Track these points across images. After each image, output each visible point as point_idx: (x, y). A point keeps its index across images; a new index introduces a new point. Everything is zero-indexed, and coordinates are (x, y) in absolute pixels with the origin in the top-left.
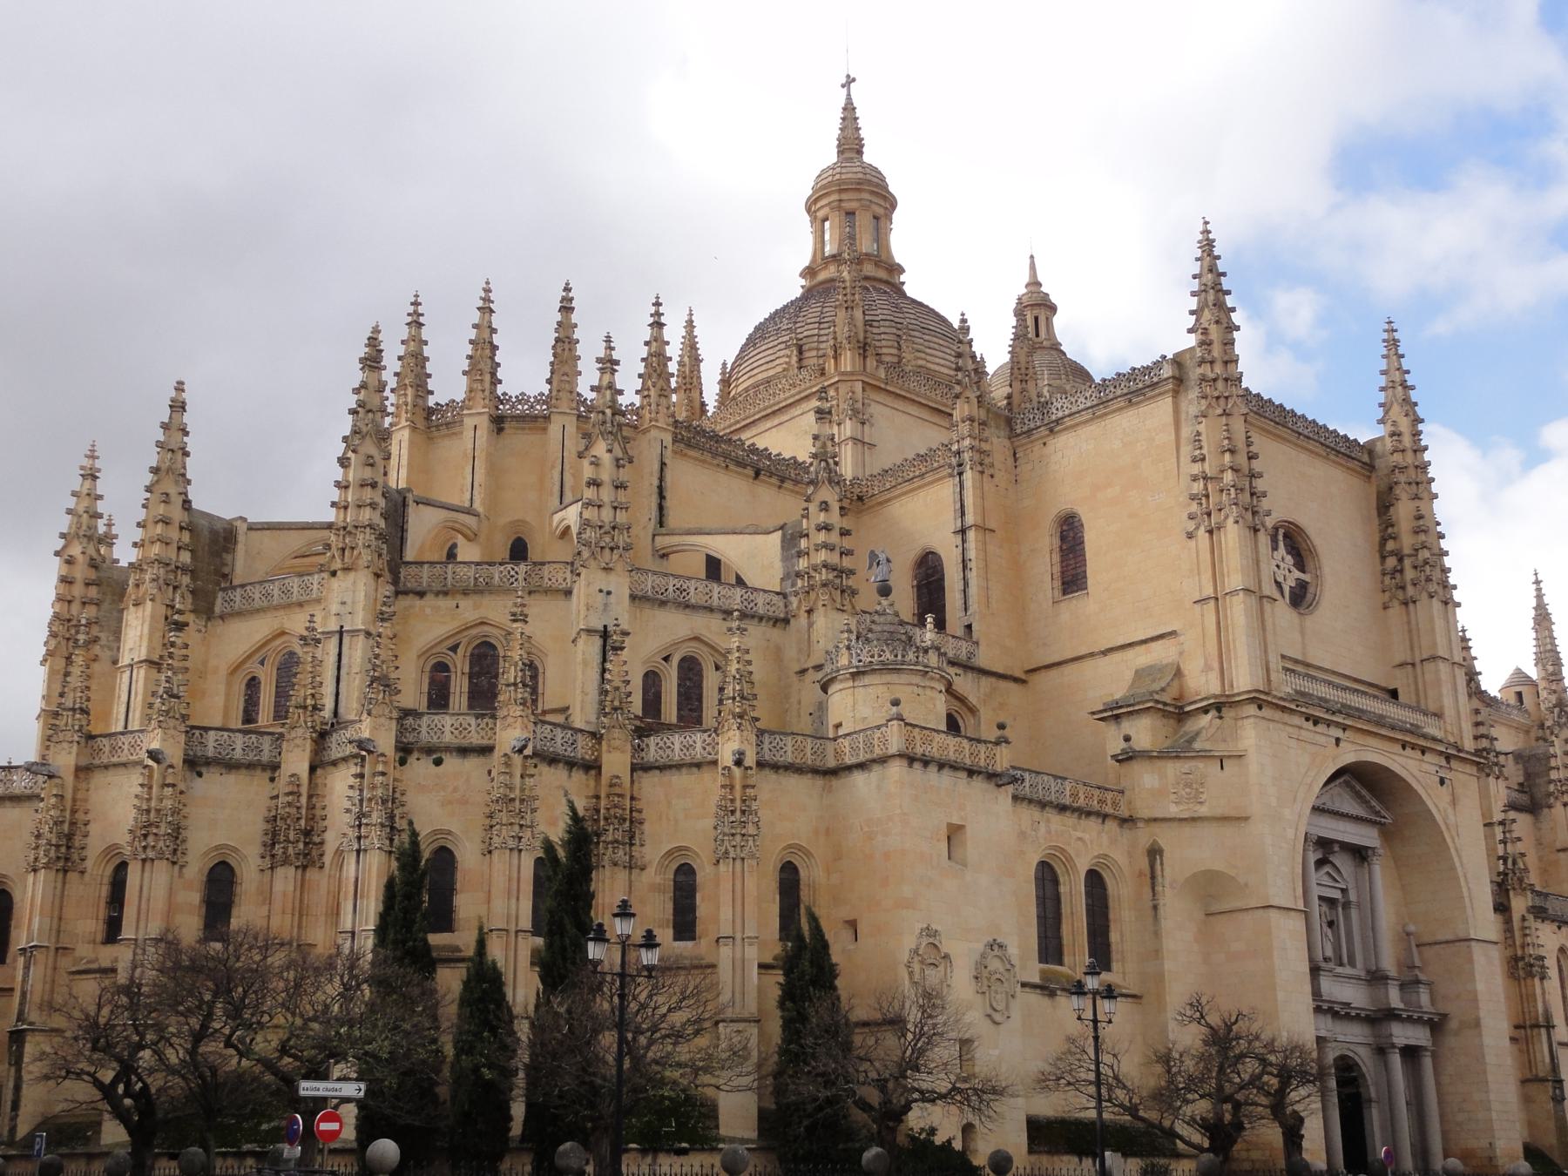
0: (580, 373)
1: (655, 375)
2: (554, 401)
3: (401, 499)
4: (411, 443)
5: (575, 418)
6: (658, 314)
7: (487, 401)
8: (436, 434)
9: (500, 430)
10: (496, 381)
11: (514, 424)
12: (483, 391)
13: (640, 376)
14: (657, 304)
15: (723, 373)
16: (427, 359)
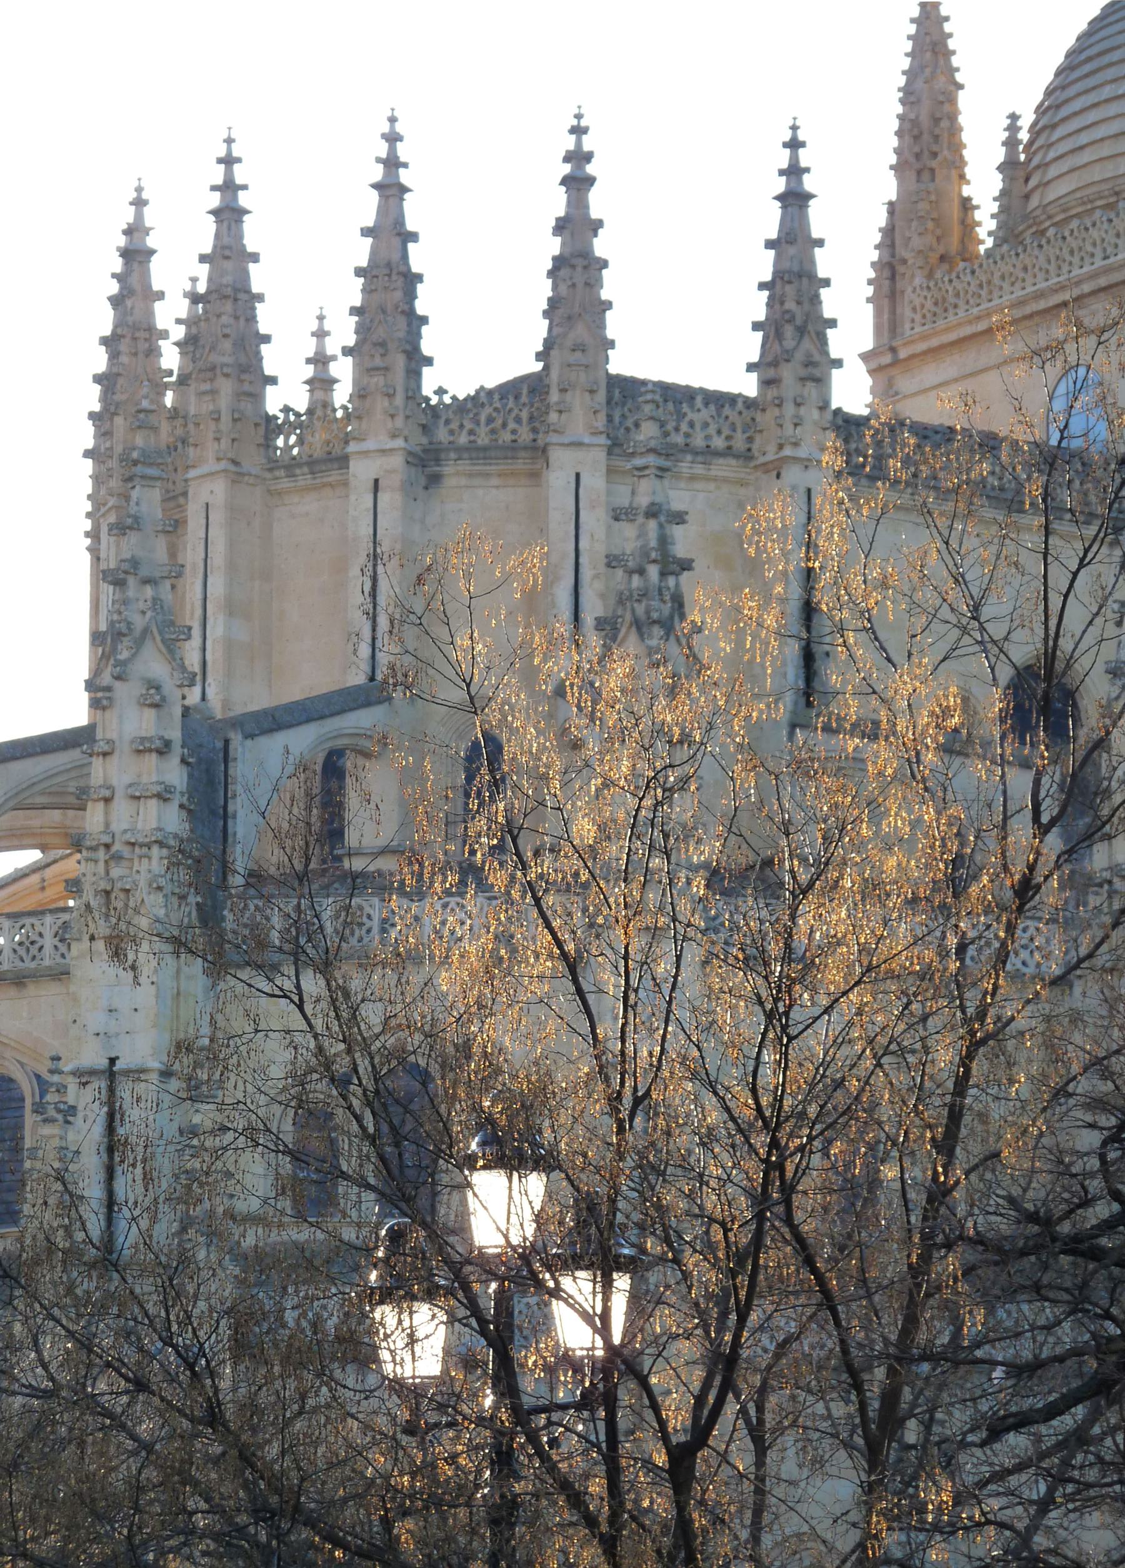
0: (611, 344)
1: (789, 331)
2: (553, 417)
3: (220, 745)
4: (234, 511)
5: (601, 455)
6: (794, 171)
7: (399, 422)
8: (285, 484)
9: (434, 480)
10: (417, 361)
11: (464, 466)
12: (390, 396)
13: (756, 326)
14: (794, 145)
15: (1011, 143)
16: (260, 298)
